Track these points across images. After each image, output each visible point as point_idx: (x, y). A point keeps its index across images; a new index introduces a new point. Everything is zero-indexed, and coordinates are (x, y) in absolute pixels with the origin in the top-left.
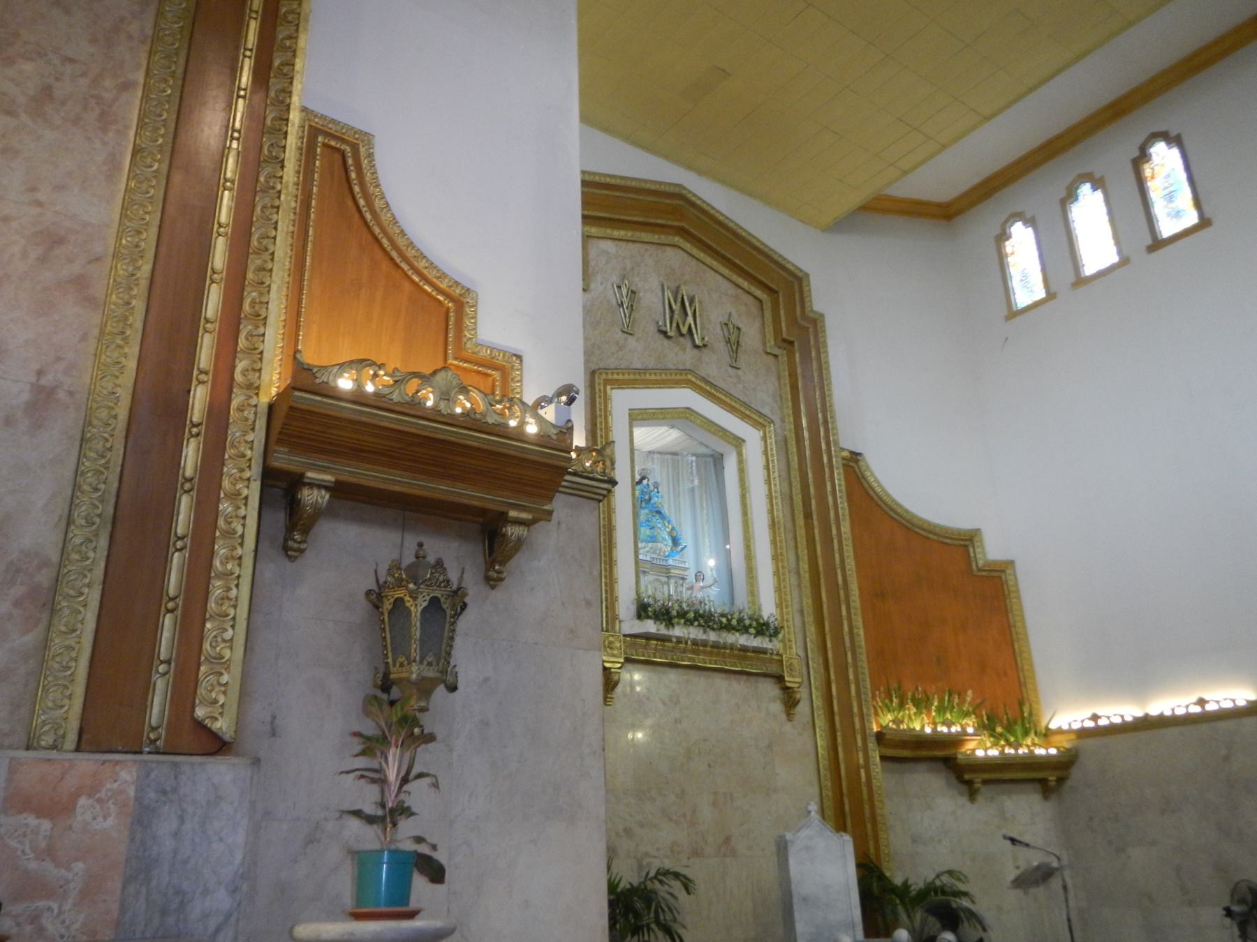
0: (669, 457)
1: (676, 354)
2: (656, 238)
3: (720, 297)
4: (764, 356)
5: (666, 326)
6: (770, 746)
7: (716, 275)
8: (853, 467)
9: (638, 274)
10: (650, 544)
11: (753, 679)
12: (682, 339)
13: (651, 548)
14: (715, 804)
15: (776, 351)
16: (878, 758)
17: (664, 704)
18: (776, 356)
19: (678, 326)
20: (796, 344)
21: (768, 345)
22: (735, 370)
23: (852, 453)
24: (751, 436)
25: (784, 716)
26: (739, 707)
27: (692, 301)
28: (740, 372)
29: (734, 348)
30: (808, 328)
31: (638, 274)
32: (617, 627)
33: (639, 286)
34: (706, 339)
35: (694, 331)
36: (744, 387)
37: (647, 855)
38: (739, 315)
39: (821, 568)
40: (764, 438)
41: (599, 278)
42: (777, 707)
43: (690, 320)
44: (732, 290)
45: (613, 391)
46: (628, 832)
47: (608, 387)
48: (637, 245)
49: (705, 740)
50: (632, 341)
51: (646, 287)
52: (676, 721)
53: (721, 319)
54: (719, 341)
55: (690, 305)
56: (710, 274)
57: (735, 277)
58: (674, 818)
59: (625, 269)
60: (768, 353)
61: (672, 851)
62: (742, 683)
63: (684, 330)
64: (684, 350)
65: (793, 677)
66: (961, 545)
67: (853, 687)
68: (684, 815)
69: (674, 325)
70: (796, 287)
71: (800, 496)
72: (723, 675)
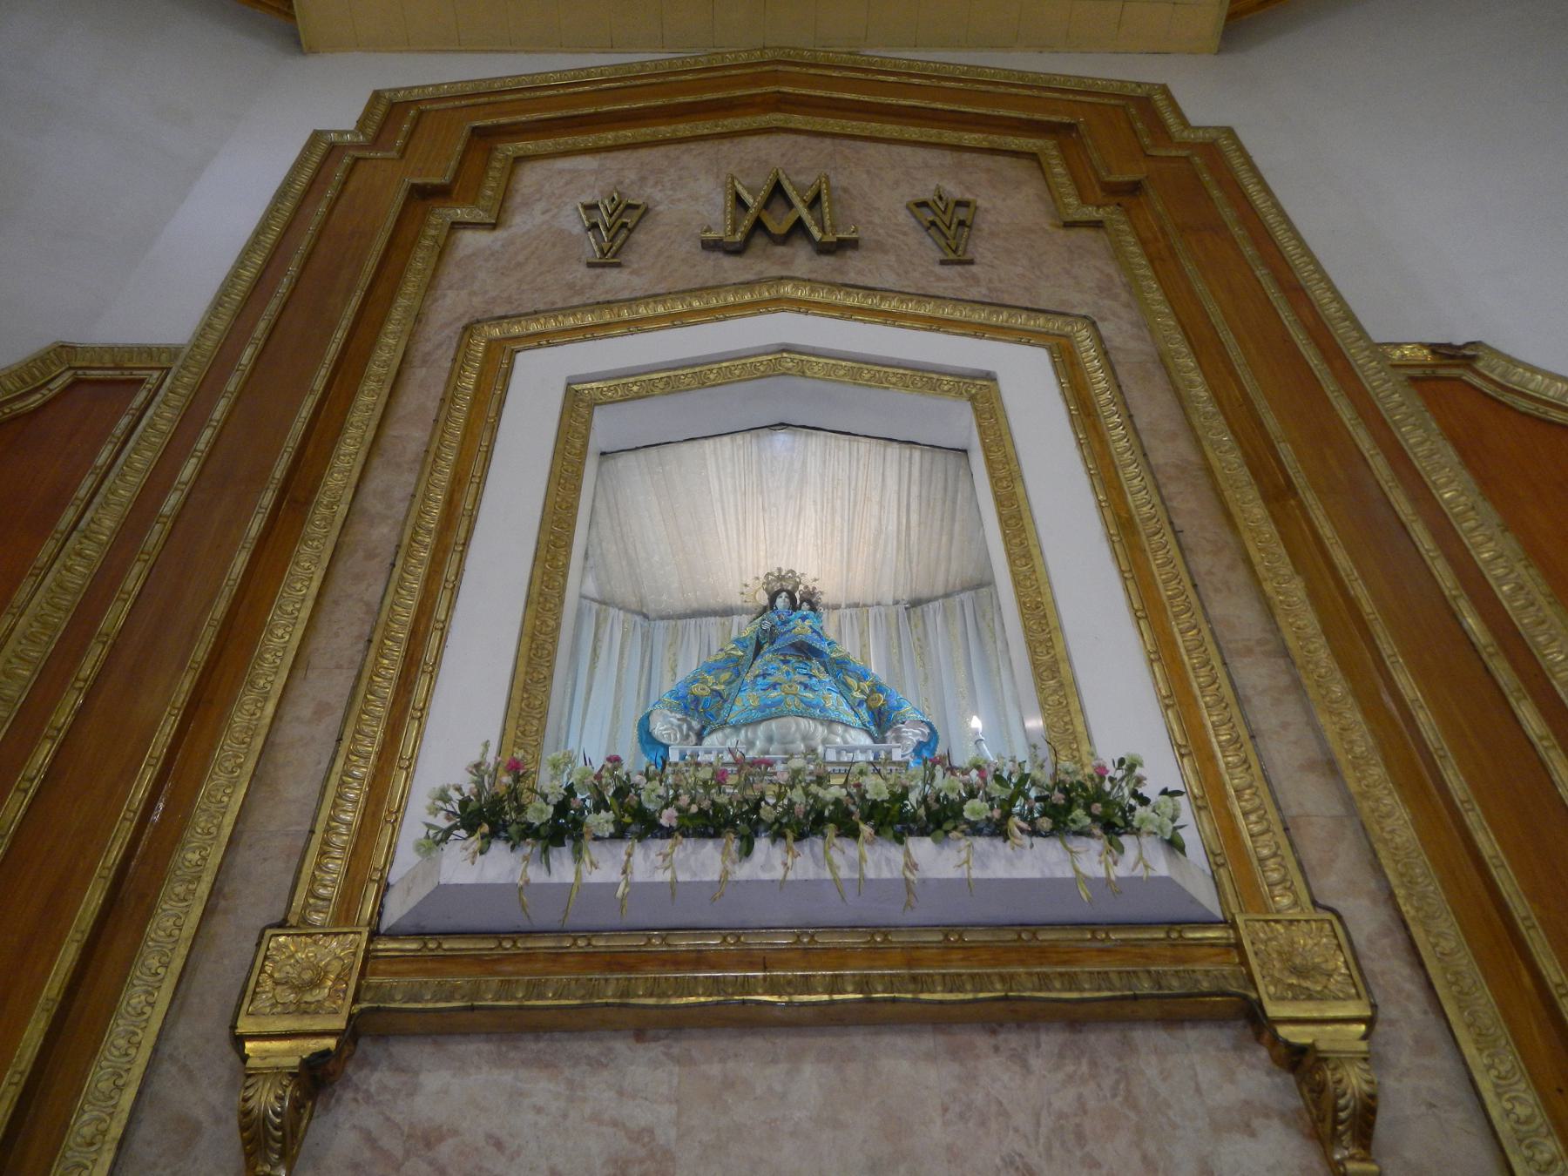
0: (966, 597)
2: (704, 128)
4: (1062, 232)
7: (895, 149)
8: (1458, 379)
10: (762, 728)
11: (1101, 1041)
12: (780, 250)
13: (770, 740)
15: (1092, 213)
18: (1097, 225)
23: (1434, 348)
28: (973, 268)
33: (658, 196)
36: (989, 289)
39: (1367, 607)
41: (539, 207)
44: (949, 158)
48: (662, 150)
53: (908, 199)
54: (905, 234)
56: (871, 149)
57: (949, 136)
60: (1069, 225)
62: (1036, 1063)
65: (1321, 997)
71: (1238, 453)
72: (928, 1042)
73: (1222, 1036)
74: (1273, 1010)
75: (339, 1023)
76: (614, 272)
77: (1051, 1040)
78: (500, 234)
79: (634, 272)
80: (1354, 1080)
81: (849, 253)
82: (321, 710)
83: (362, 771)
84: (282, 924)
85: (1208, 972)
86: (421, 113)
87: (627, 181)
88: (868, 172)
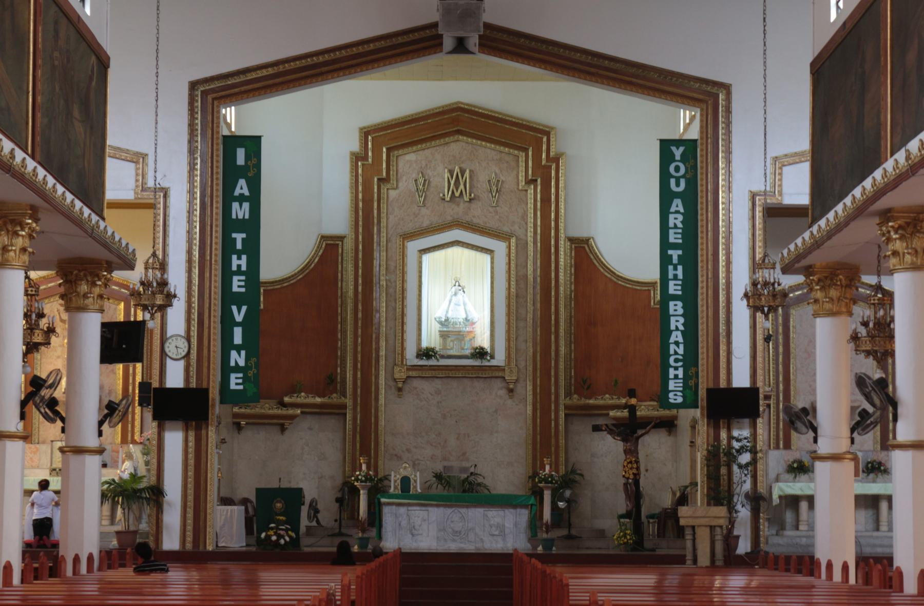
1: (453, 209)
3: (488, 164)
5: (444, 195)
6: (496, 411)
9: (430, 167)
11: (488, 379)
12: (458, 199)
14: (458, 439)
16: (563, 415)
17: (432, 395)
19: (453, 192)
20: (539, 181)
21: (520, 185)
22: (494, 208)
24: (500, 247)
25: (507, 396)
26: (478, 394)
27: (463, 172)
28: (498, 208)
29: (494, 194)
30: (551, 166)
31: (430, 167)
32: (405, 363)
33: (430, 174)
34: (473, 195)
35: (464, 193)
37: (418, 459)
38: (501, 171)
40: (509, 247)
41: (404, 178)
42: (503, 392)
43: (462, 187)
45: (409, 243)
46: (408, 450)
47: (406, 241)
48: (431, 149)
49: (455, 410)
50: (424, 211)
51: (435, 174)
52: (438, 403)
54: (484, 192)
55: (462, 177)
58: (434, 444)
59: (421, 167)
61: (432, 458)
63: (457, 194)
64: (458, 205)
66: (646, 290)
67: (553, 379)
68: (440, 444)
69: (450, 193)
70: (545, 139)
72: (469, 379)
73: (502, 379)
74: (506, 378)
75: (405, 377)
76: (422, 208)
77: (483, 379)
78: (397, 191)
79: (427, 208)
80: (511, 386)
81: (472, 201)
82: (391, 328)
83: (400, 341)
84: (395, 365)
85: (500, 374)
86: (373, 138)
87: (423, 166)
88: (479, 163)
